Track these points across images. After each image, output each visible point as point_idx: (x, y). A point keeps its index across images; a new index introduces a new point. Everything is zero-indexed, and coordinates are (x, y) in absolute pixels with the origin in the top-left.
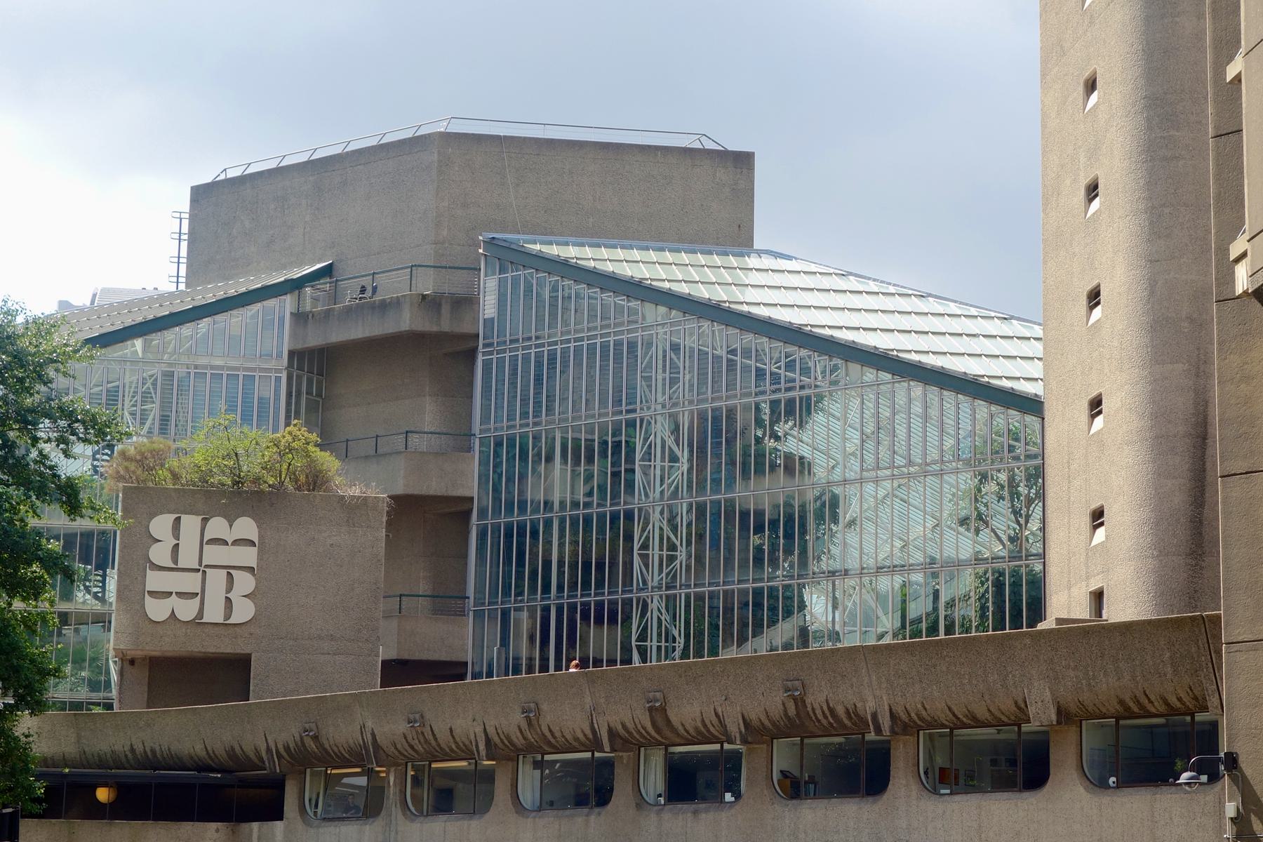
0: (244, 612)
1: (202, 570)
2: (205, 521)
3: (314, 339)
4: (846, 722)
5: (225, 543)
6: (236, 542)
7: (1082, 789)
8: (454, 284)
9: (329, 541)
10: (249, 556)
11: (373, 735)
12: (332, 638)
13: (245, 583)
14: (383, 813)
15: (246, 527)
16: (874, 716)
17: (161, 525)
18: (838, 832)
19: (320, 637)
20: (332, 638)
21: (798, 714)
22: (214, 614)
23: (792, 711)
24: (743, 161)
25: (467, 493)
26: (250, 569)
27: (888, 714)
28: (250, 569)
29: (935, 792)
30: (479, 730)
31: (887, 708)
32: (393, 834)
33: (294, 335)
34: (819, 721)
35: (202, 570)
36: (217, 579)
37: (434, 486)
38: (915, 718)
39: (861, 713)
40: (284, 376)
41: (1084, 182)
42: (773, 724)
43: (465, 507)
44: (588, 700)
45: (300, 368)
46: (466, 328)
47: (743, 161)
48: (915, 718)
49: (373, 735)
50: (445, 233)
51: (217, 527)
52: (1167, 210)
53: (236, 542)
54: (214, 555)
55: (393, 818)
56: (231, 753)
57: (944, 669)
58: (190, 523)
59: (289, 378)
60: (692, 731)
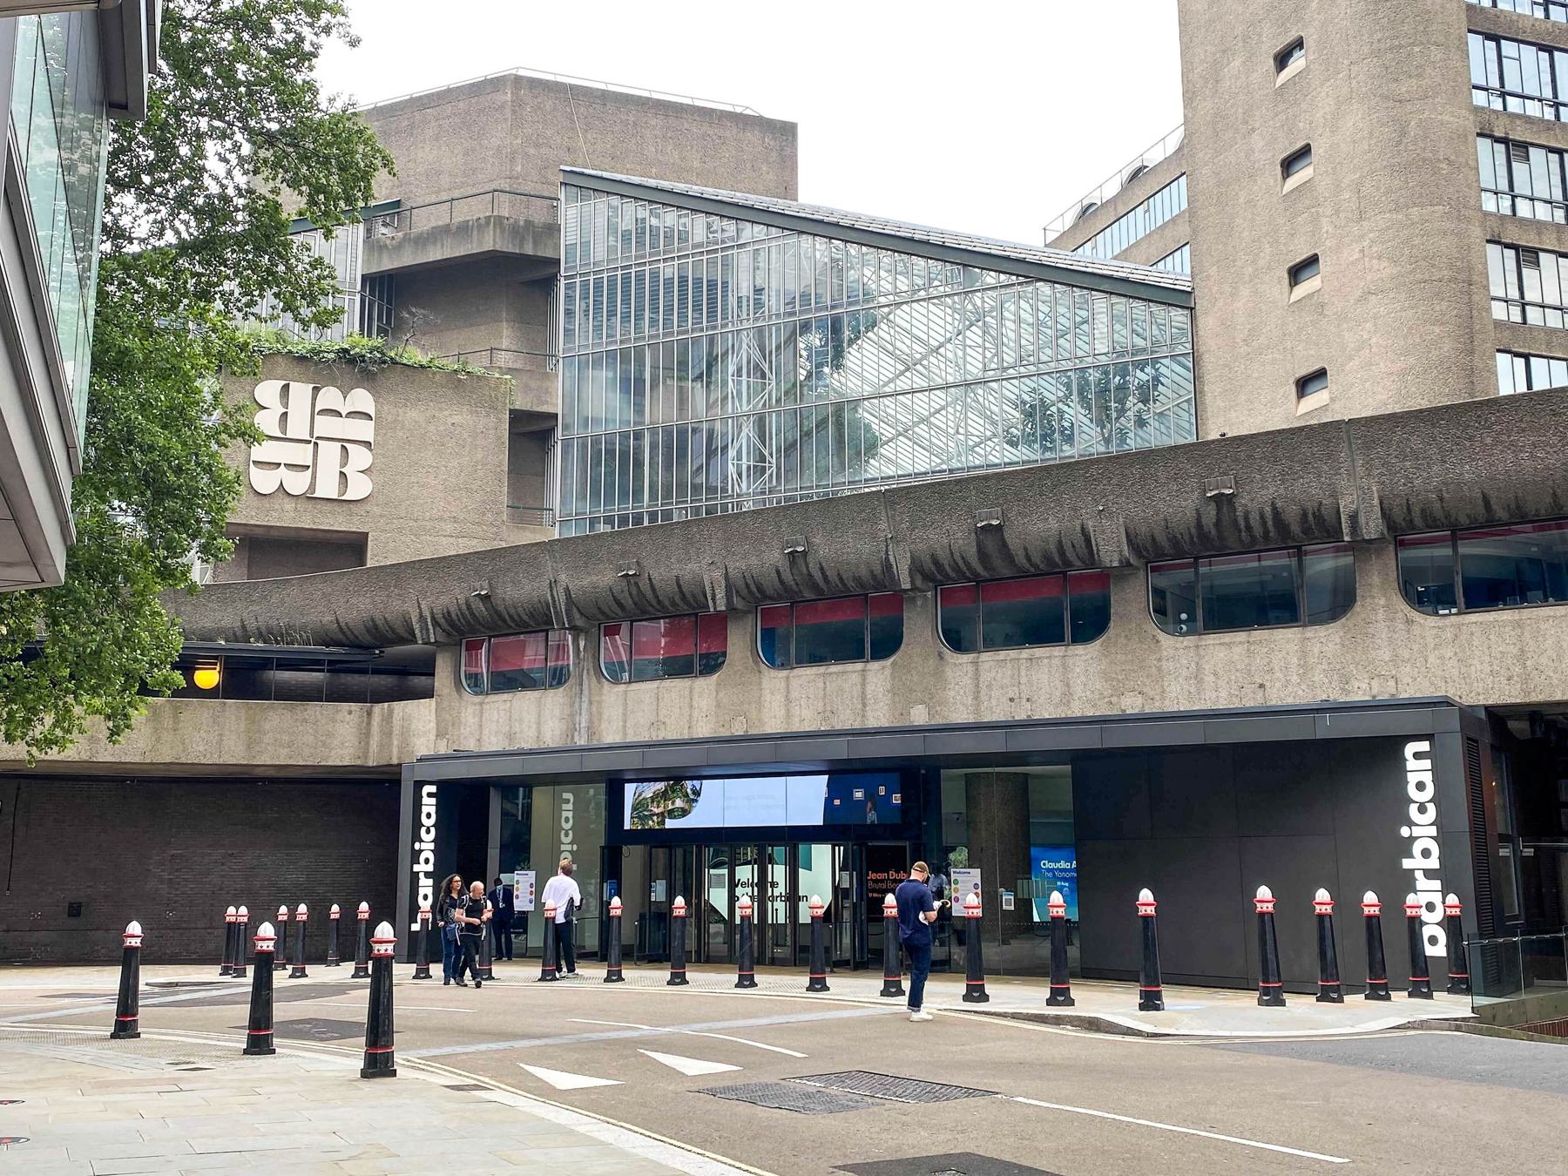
0: (359, 488)
2: (316, 390)
3: (387, 264)
4: (1295, 528)
6: (350, 415)
9: (450, 421)
10: (365, 430)
11: (567, 590)
12: (455, 520)
13: (360, 458)
14: (572, 681)
15: (362, 399)
16: (1354, 518)
17: (267, 391)
18: (1271, 671)
19: (441, 519)
20: (455, 520)
21: (1218, 524)
22: (327, 488)
24: (785, 133)
25: (551, 410)
26: (367, 444)
28: (367, 444)
30: (718, 574)
31: (1376, 502)
32: (585, 706)
33: (366, 262)
34: (1249, 528)
35: (314, 442)
36: (330, 452)
39: (1327, 513)
40: (358, 298)
43: (546, 425)
44: (883, 526)
46: (549, 254)
47: (785, 133)
49: (567, 590)
50: (519, 168)
51: (330, 396)
53: (350, 415)
54: (325, 426)
55: (585, 687)
57: (1489, 440)
58: (301, 391)
60: (1037, 559)
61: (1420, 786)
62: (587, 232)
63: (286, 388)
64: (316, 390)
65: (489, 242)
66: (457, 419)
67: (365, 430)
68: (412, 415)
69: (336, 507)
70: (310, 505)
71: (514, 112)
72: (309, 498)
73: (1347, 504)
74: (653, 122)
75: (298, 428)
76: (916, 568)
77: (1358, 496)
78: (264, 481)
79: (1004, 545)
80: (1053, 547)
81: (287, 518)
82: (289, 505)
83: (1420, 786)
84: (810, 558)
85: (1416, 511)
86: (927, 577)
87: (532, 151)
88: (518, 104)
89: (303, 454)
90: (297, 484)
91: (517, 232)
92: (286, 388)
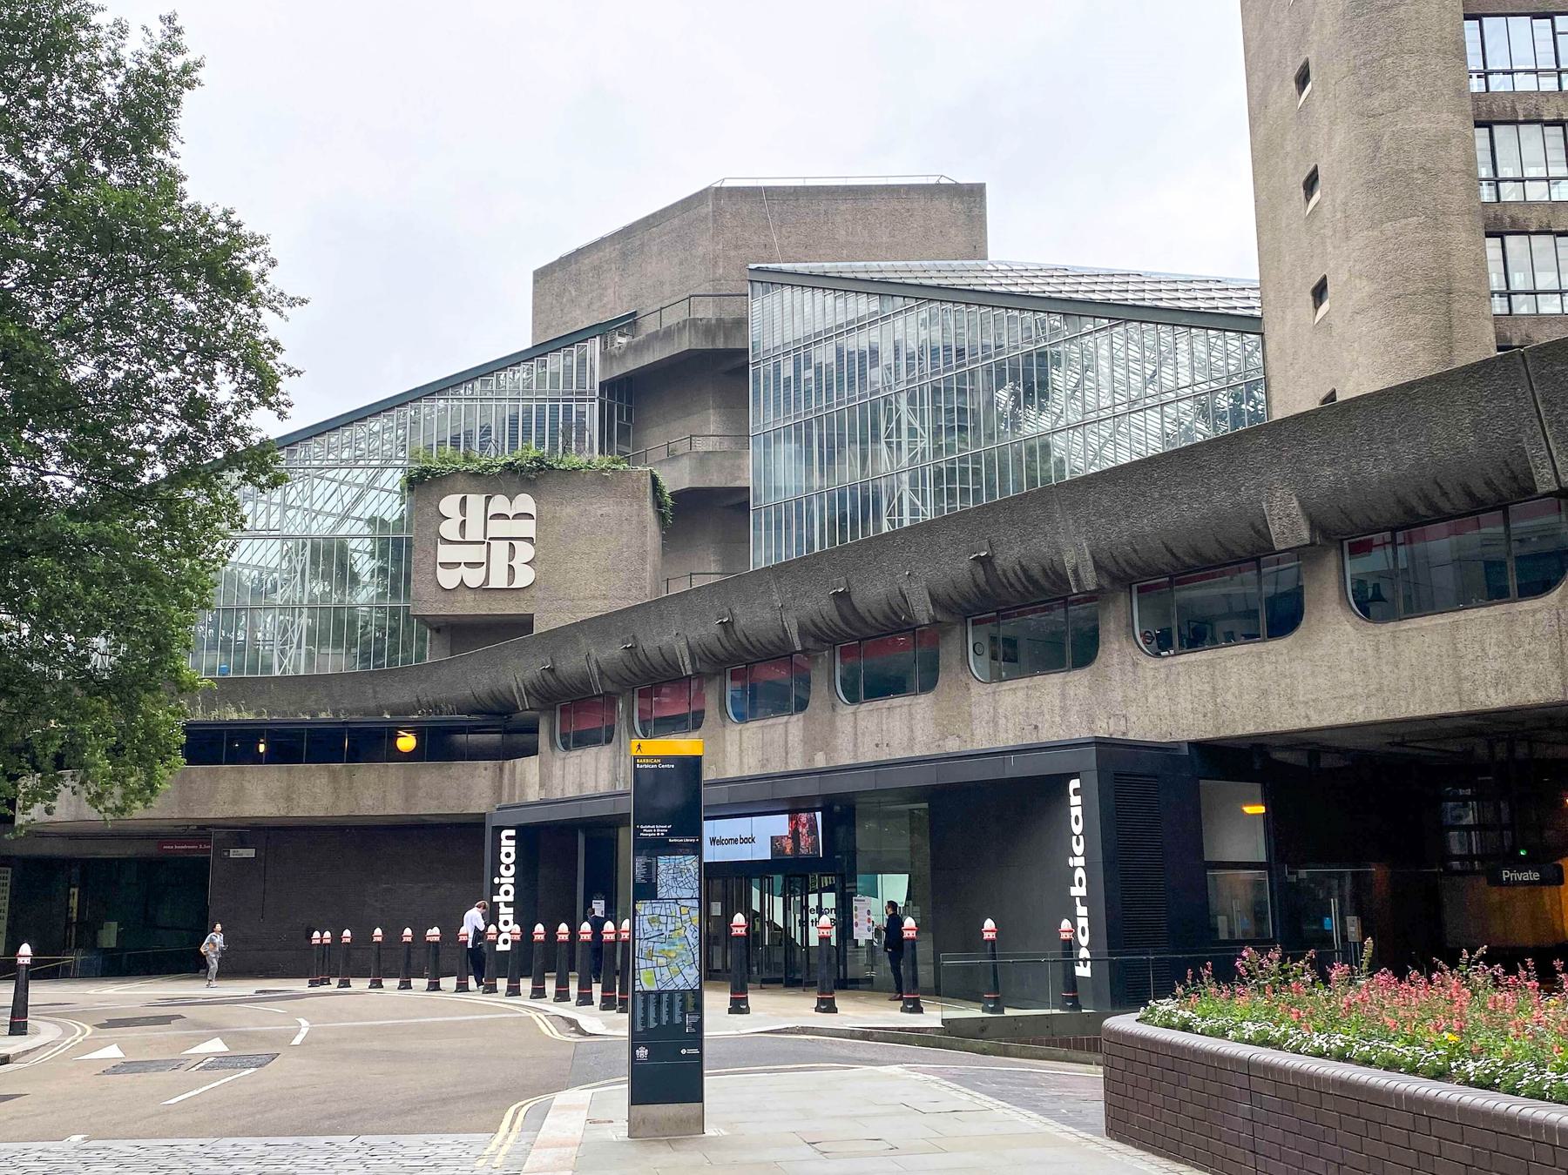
0: (524, 577)
1: (487, 542)
2: (488, 499)
3: (617, 371)
4: (1043, 581)
5: (506, 517)
6: (516, 516)
7: (1349, 628)
8: (730, 311)
10: (528, 528)
15: (525, 503)
16: (1075, 571)
17: (449, 505)
18: (1042, 714)
19: (594, 597)
20: (605, 597)
22: (499, 580)
23: (981, 576)
24: (975, 193)
27: (1090, 563)
29: (1158, 655)
30: (683, 644)
31: (1088, 556)
33: (603, 370)
34: (1012, 585)
35: (487, 542)
36: (500, 549)
37: (716, 480)
38: (1124, 564)
40: (596, 404)
41: (1292, 72)
42: (963, 597)
45: (611, 396)
46: (739, 346)
47: (975, 193)
48: (1124, 564)
51: (499, 503)
52: (1389, 61)
53: (516, 516)
54: (496, 528)
56: (493, 697)
57: (1156, 495)
58: (476, 501)
59: (601, 404)
60: (880, 618)
61: (508, 855)
62: (780, 322)
63: (464, 500)
64: (488, 499)
65: (685, 343)
66: (604, 510)
67: (528, 528)
68: (568, 511)
69: (508, 595)
70: (486, 595)
71: (715, 221)
72: (484, 589)
73: (1069, 559)
74: (842, 208)
75: (474, 532)
76: (803, 632)
77: (1074, 550)
78: (448, 579)
79: (854, 609)
80: (886, 608)
81: (468, 607)
82: (470, 596)
83: (508, 855)
84: (736, 627)
85: (1121, 560)
86: (817, 639)
87: (733, 253)
88: (718, 213)
89: (477, 553)
90: (474, 578)
91: (709, 330)
92: (464, 500)
